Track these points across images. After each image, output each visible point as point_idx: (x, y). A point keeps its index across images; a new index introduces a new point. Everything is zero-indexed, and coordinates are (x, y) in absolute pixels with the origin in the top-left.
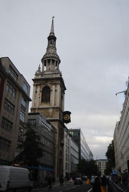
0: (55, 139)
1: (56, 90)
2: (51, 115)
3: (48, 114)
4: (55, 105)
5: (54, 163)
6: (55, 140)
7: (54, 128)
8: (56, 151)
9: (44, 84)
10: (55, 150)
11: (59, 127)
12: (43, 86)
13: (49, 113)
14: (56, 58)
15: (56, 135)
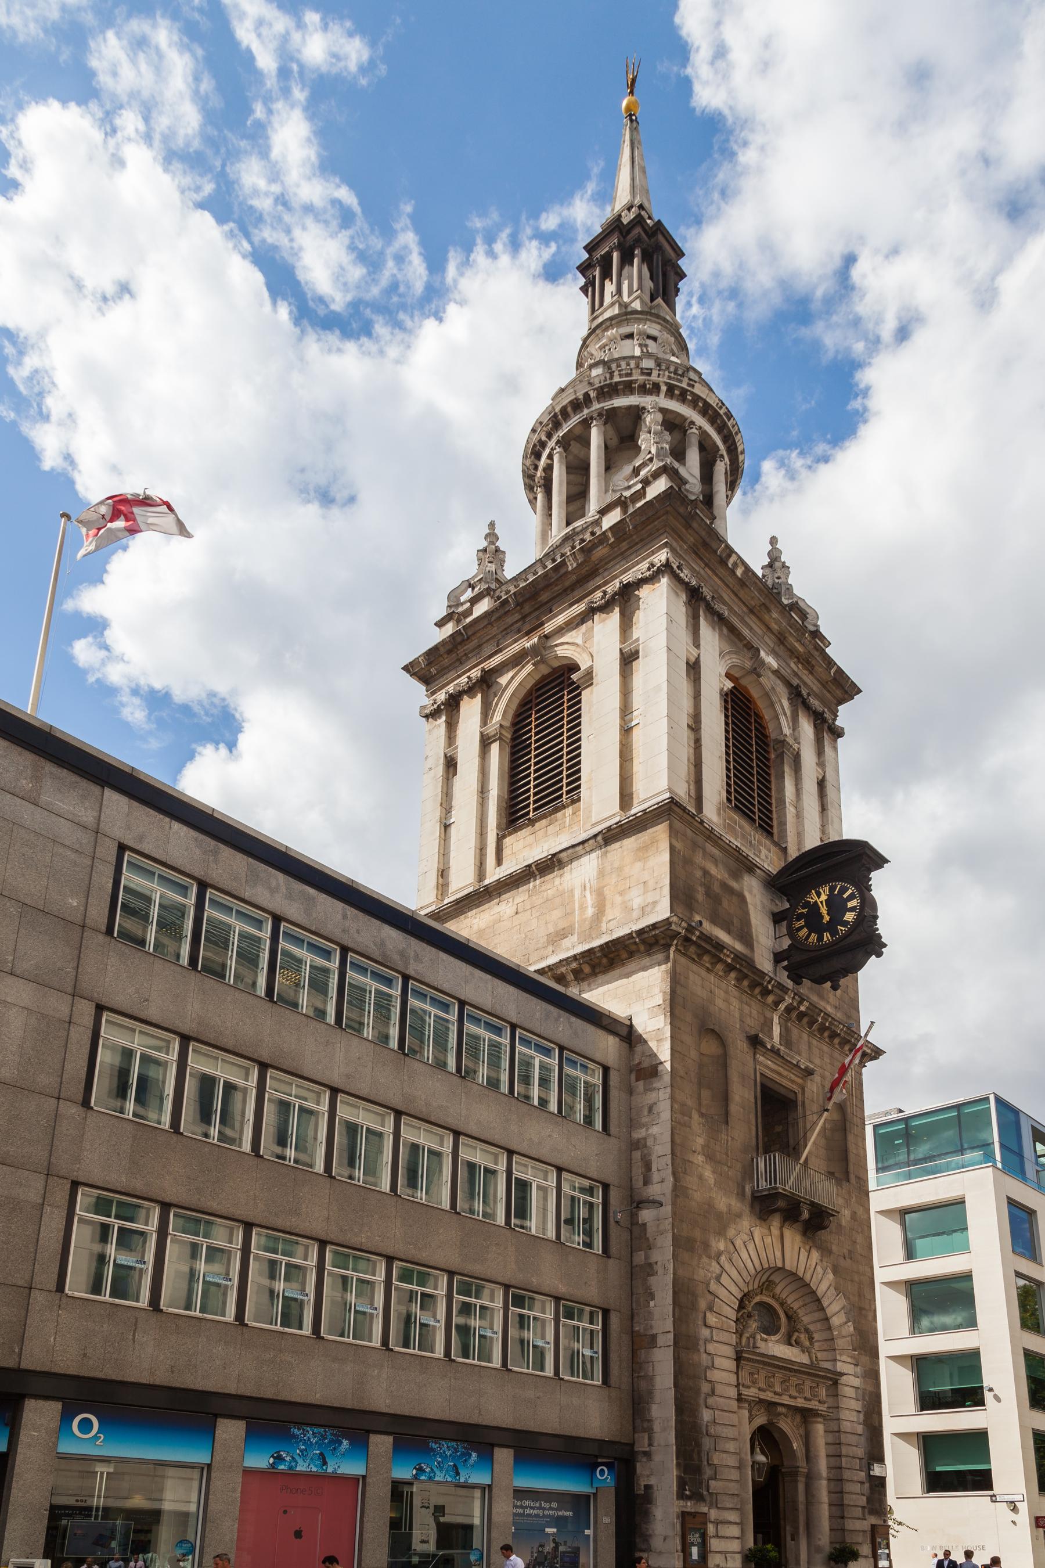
0: (637, 1145)
1: (628, 659)
2: (590, 912)
3: (557, 914)
4: (626, 798)
5: (637, 1405)
6: (637, 1155)
7: (628, 1035)
8: (649, 1269)
9: (517, 661)
10: (640, 1258)
11: (677, 1003)
12: (512, 683)
13: (565, 898)
14: (655, 389)
15: (651, 1097)
